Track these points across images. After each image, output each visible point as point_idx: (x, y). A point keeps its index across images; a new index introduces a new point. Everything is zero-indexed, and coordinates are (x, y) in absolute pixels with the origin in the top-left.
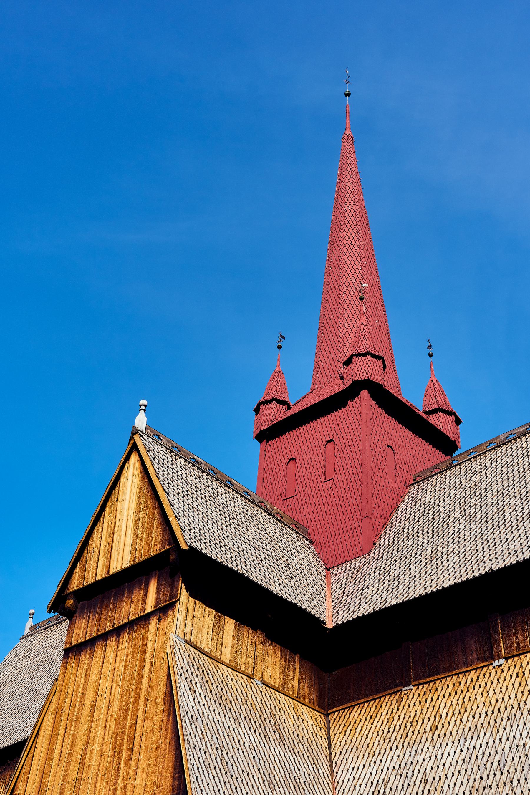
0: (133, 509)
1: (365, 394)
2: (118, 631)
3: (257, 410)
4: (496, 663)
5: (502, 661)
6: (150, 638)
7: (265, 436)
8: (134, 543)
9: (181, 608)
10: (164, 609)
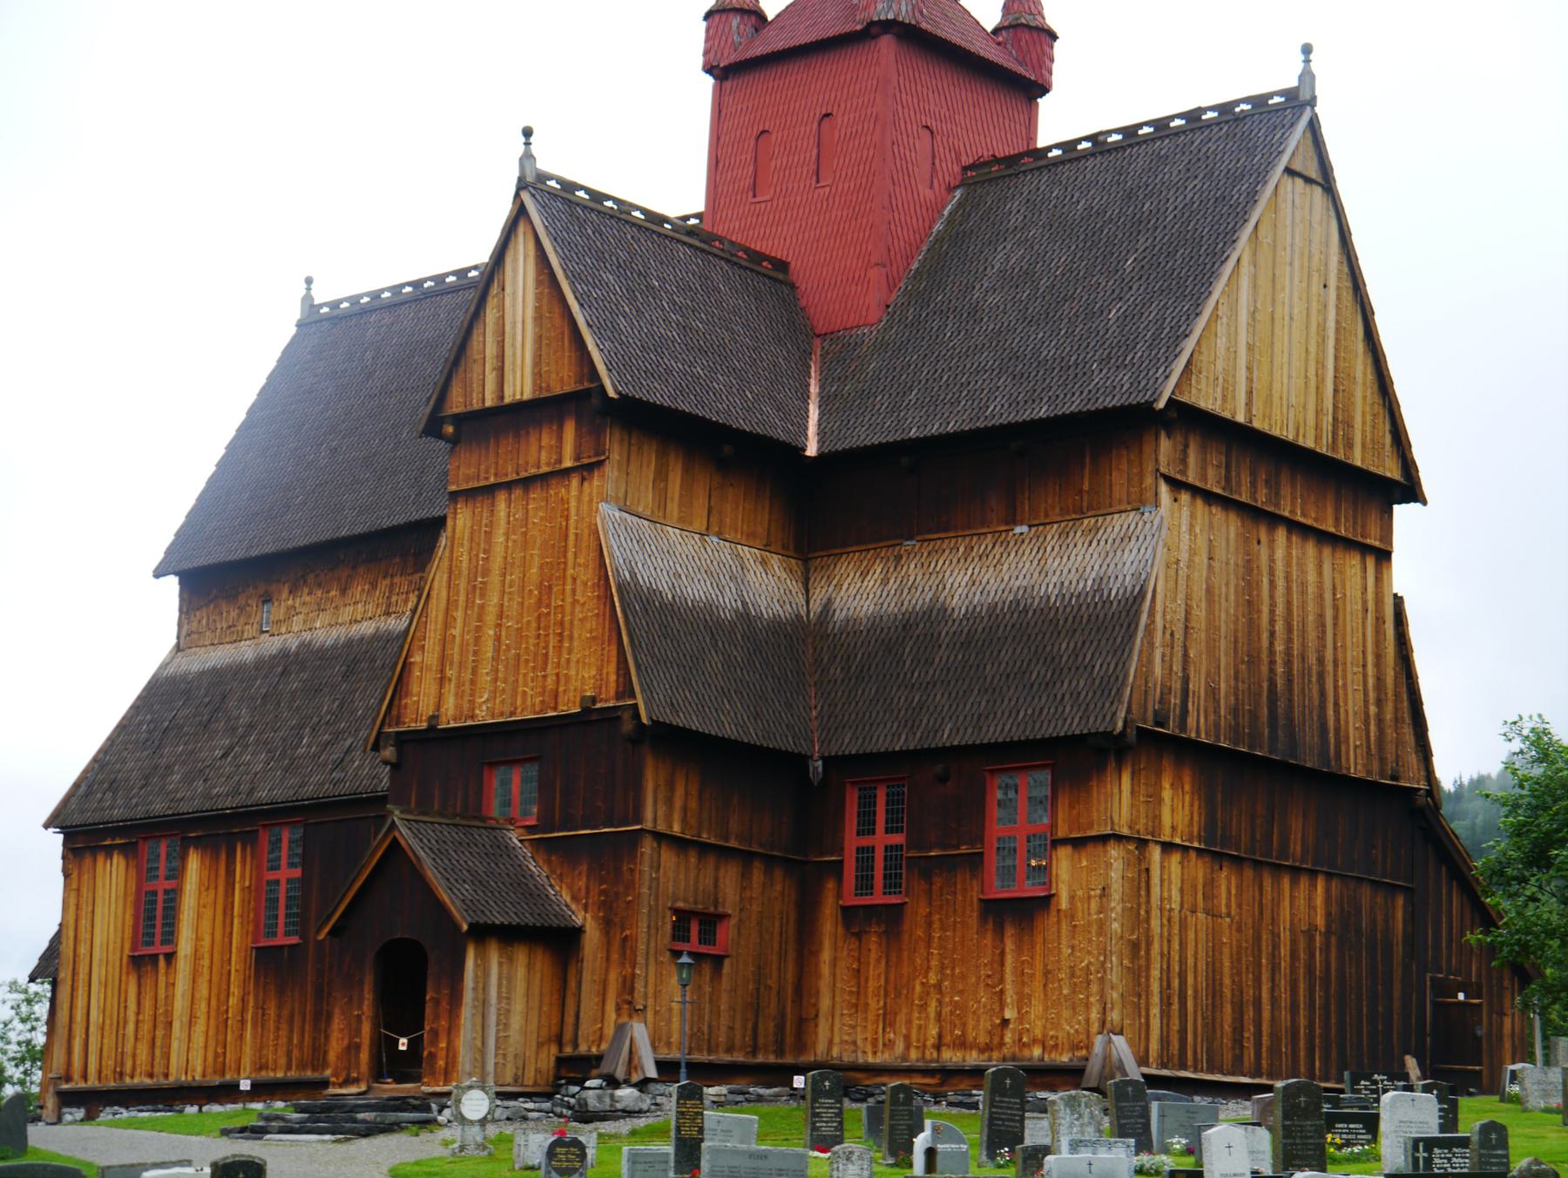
0: (530, 312)
1: (887, 43)
2: (527, 483)
3: (708, 16)
4: (1018, 530)
5: (1025, 529)
6: (573, 504)
7: (723, 71)
8: (537, 362)
9: (610, 471)
10: (586, 470)
